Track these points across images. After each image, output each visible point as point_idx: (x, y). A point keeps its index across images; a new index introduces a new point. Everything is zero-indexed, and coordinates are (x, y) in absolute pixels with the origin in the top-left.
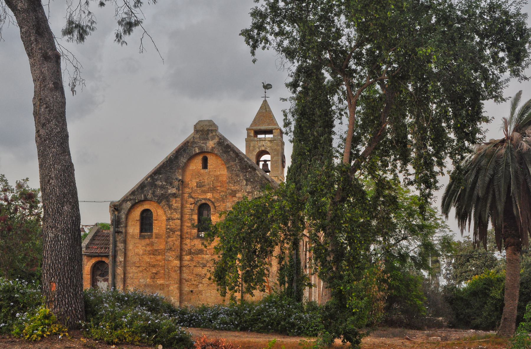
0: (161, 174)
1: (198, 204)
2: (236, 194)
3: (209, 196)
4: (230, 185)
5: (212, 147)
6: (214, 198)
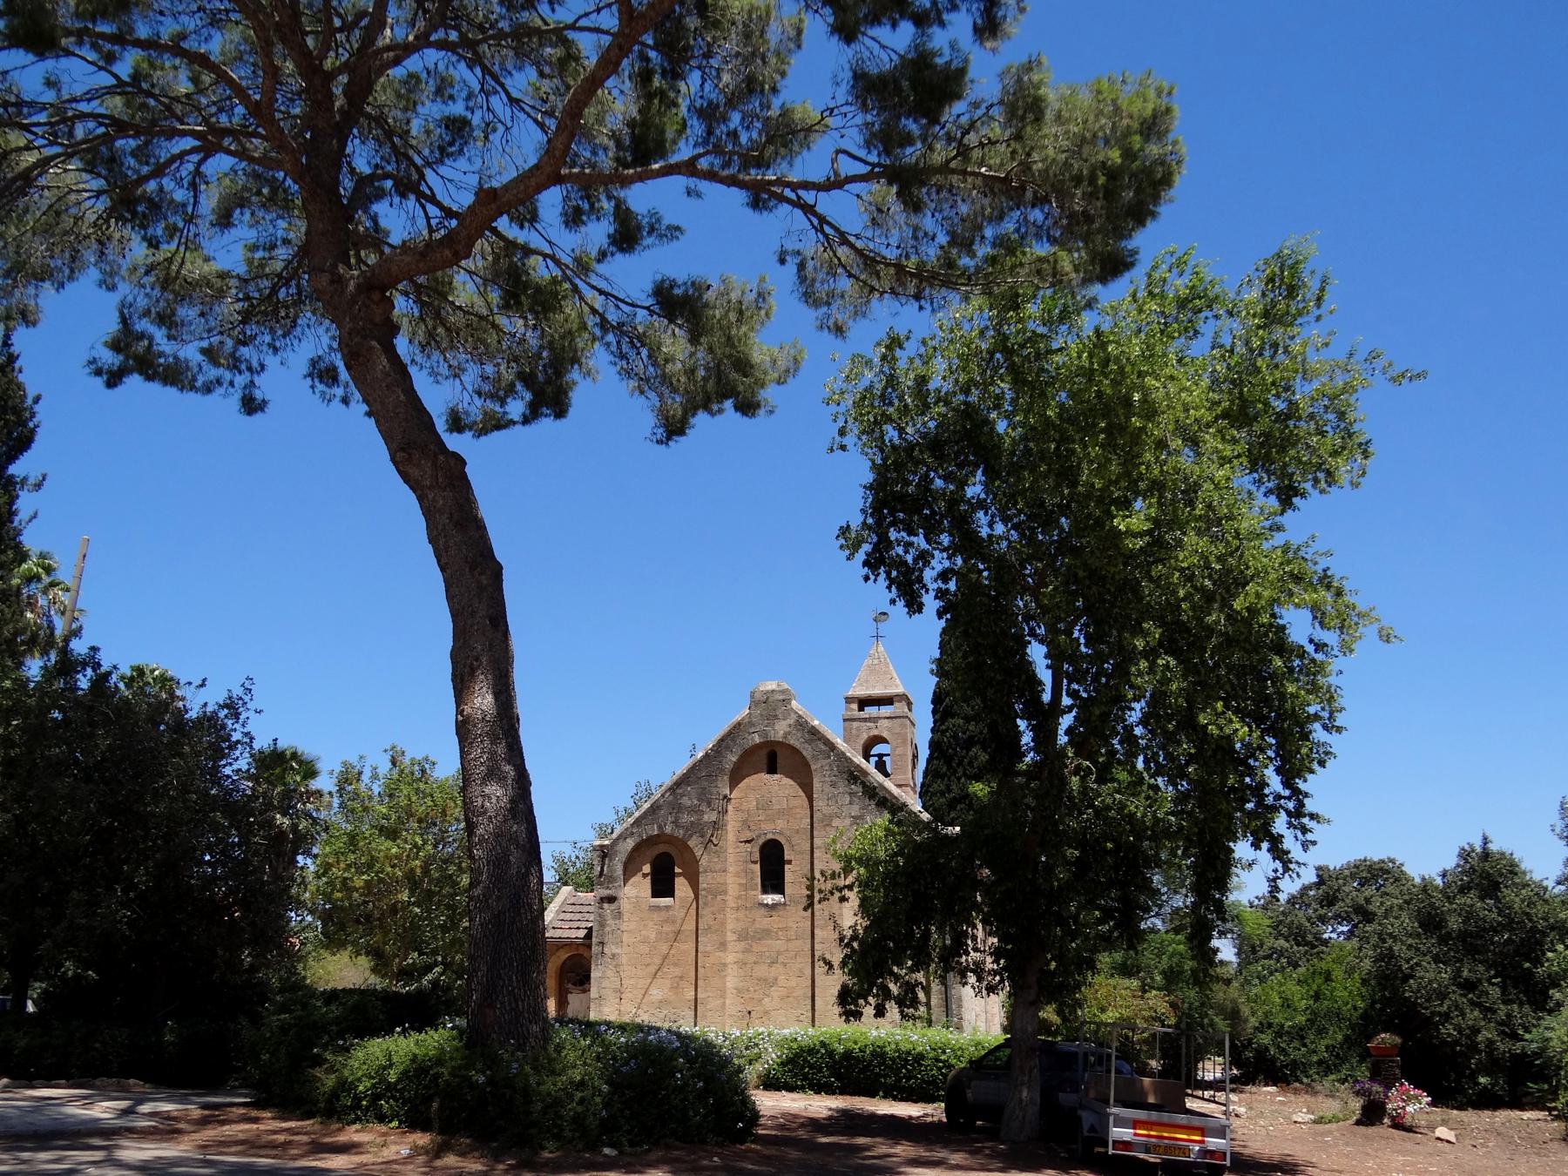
1: (761, 841)
3: (780, 824)
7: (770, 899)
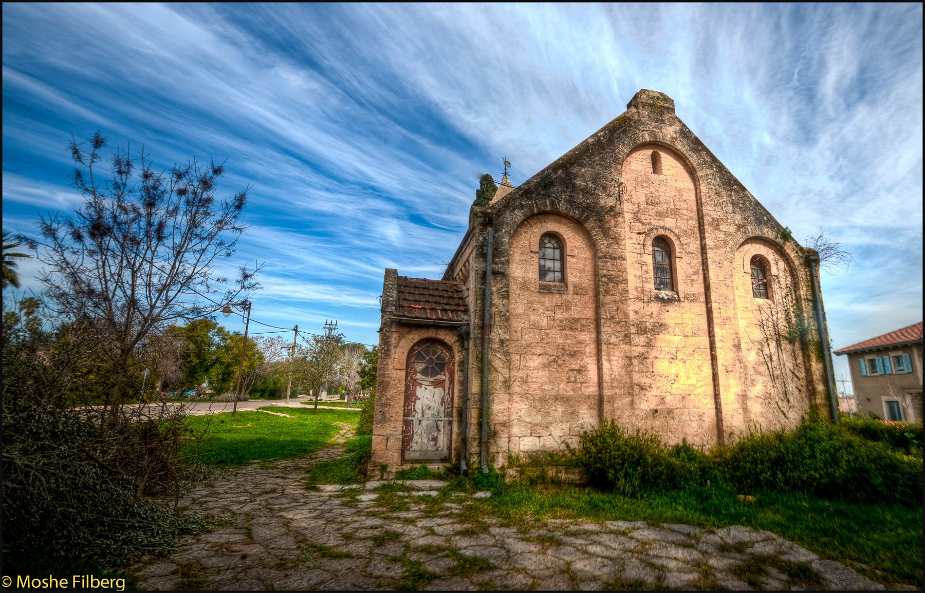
0: (583, 167)
2: (718, 225)
3: (669, 222)
4: (709, 208)
5: (672, 137)
7: (664, 294)
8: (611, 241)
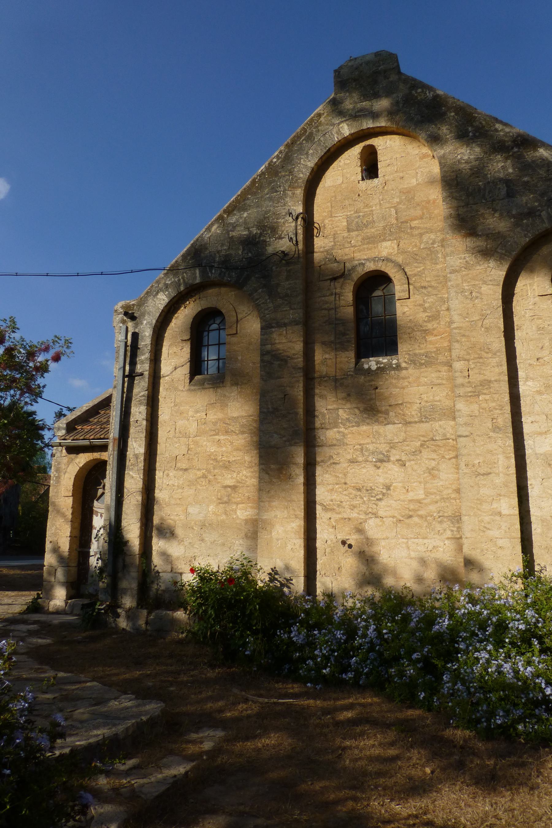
0: (245, 210)
3: (387, 248)
6: (404, 252)
8: (280, 301)
